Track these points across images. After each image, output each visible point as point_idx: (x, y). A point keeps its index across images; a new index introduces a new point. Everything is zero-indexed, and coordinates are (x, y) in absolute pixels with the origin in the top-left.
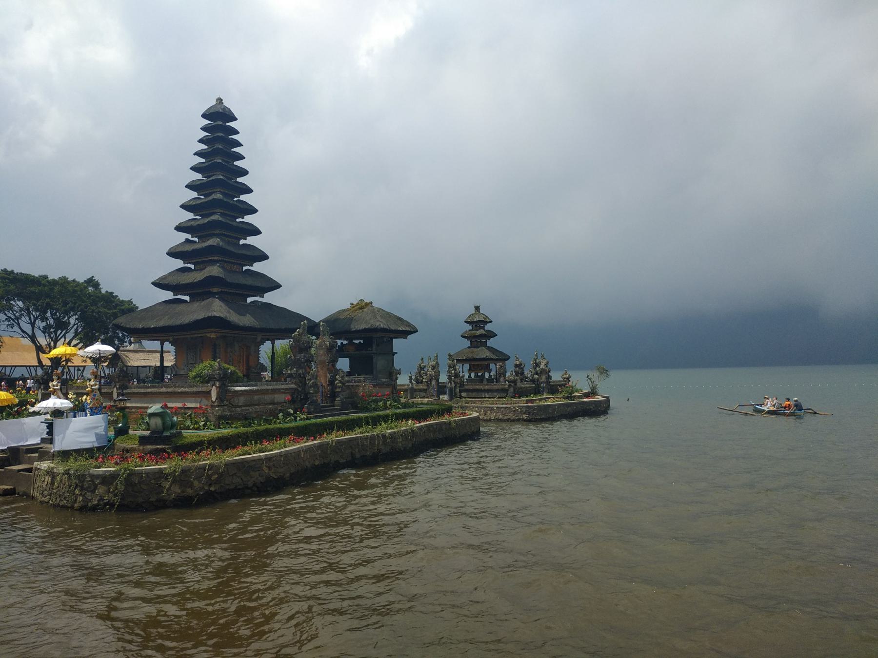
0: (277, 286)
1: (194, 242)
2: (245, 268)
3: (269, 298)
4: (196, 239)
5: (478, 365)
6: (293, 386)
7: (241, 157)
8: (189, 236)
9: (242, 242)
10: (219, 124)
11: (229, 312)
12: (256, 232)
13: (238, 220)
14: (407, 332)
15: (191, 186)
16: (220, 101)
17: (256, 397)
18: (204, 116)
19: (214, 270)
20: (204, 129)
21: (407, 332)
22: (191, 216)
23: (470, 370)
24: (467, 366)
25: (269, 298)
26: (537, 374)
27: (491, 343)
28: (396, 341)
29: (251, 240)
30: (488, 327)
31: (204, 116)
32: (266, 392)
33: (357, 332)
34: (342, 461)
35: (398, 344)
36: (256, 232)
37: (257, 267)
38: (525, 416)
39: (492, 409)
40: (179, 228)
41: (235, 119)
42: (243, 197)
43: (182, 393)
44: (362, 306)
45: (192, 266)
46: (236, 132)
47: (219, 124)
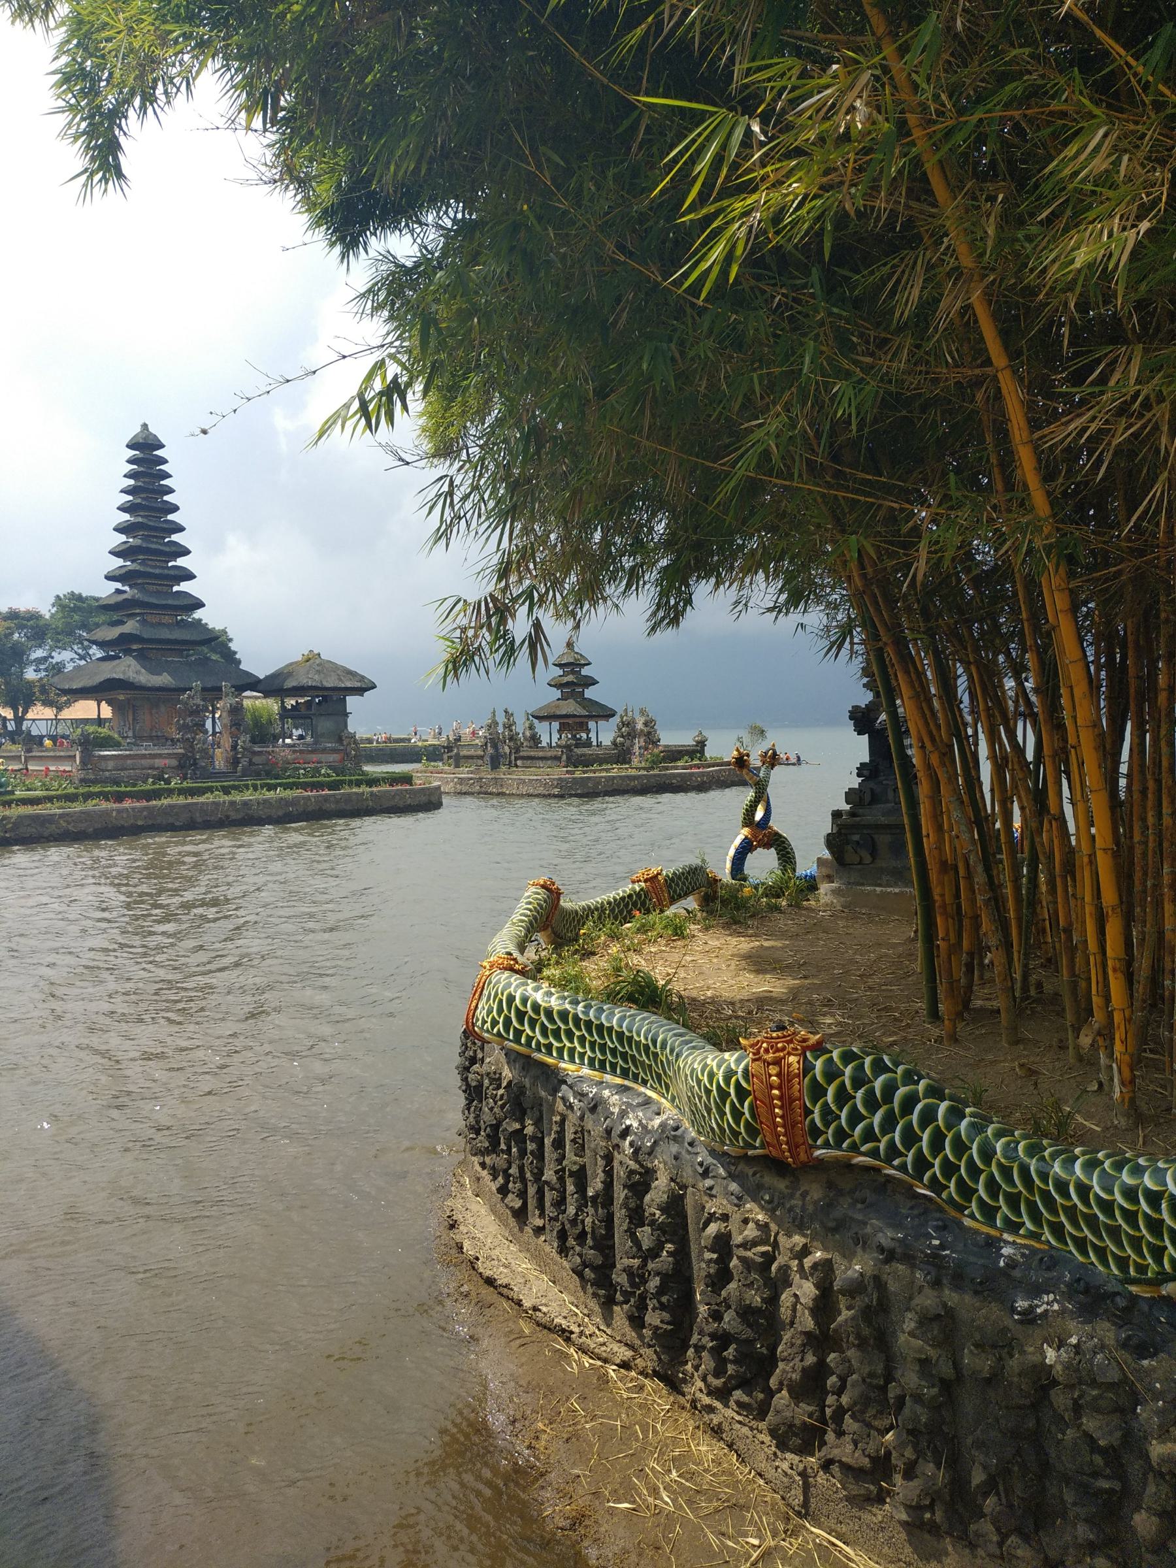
1: (125, 592)
4: (127, 588)
5: (572, 724)
6: (181, 751)
7: (170, 491)
8: (119, 585)
9: (175, 589)
10: (147, 454)
11: (138, 672)
12: (190, 576)
13: (170, 564)
14: (364, 687)
15: (119, 529)
16: (145, 426)
17: (129, 762)
18: (130, 446)
19: (130, 627)
20: (130, 461)
21: (364, 687)
22: (120, 562)
23: (560, 731)
24: (556, 725)
26: (623, 736)
27: (590, 693)
28: (350, 700)
29: (184, 586)
30: (585, 671)
31: (130, 446)
32: (144, 756)
33: (287, 690)
34: (177, 824)
35: (352, 702)
36: (190, 576)
38: (556, 791)
39: (523, 782)
40: (109, 578)
41: (162, 446)
42: (175, 537)
43: (61, 757)
44: (312, 659)
46: (165, 461)
47: (147, 454)
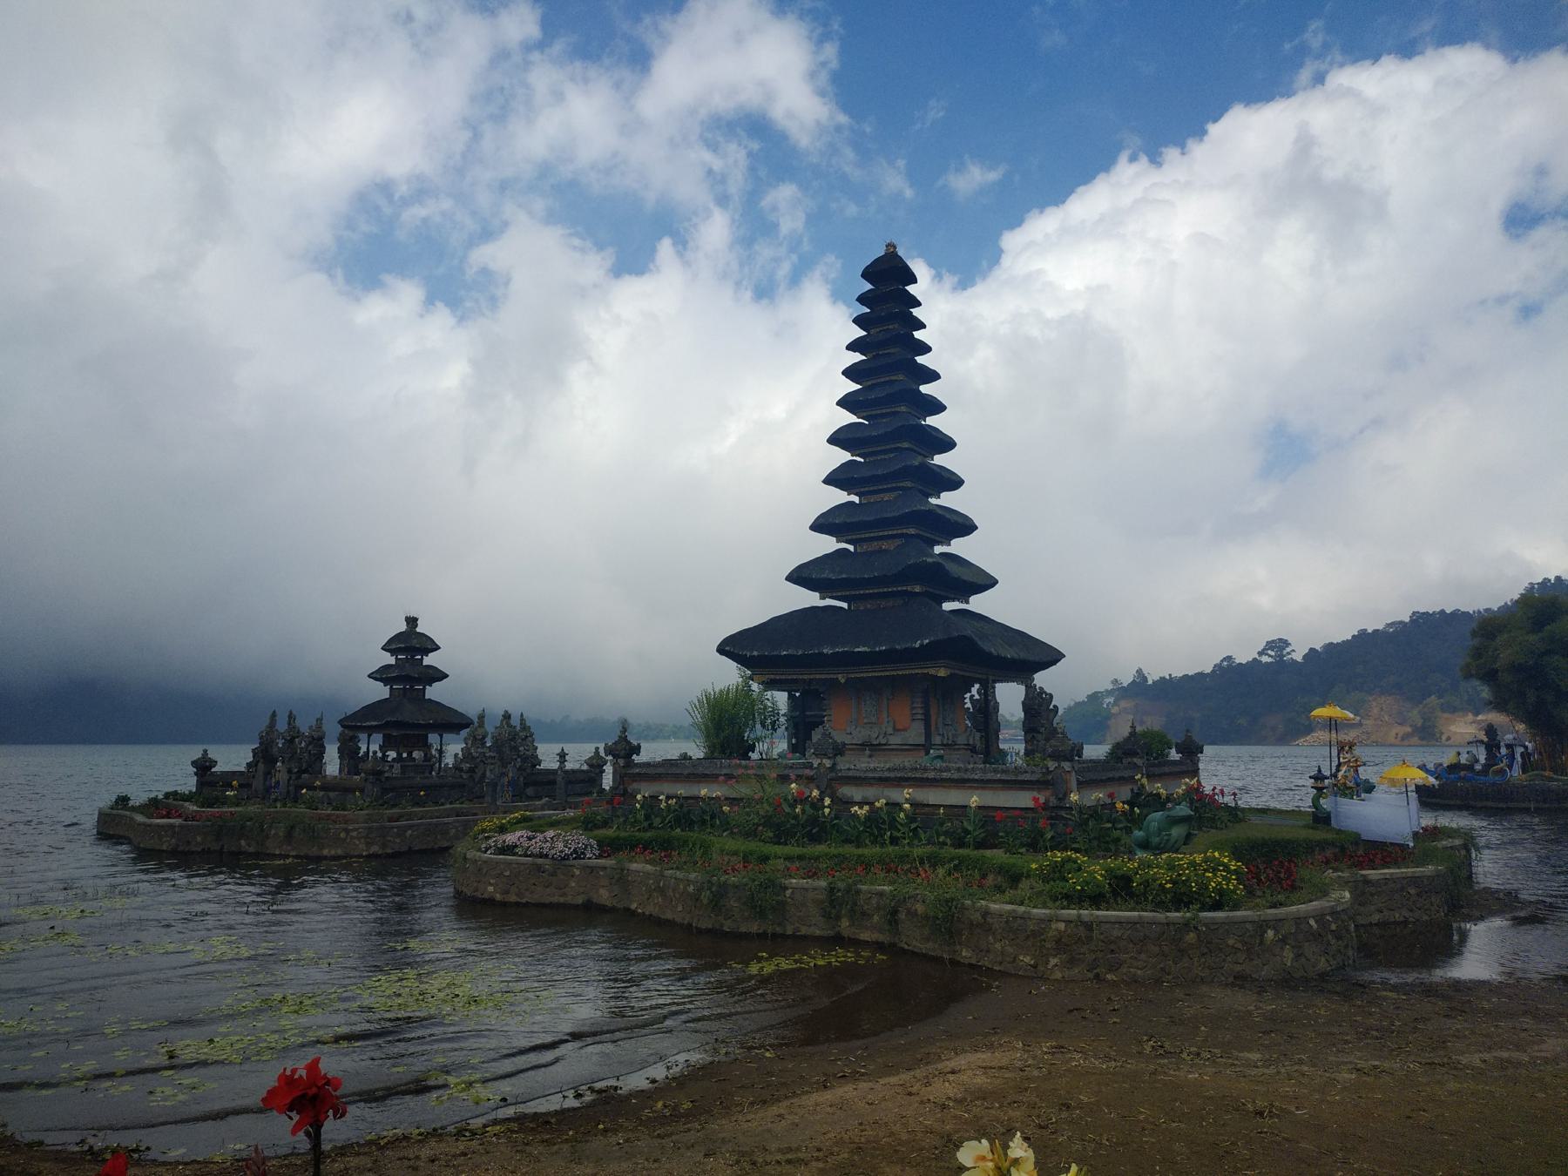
0: (991, 583)
2: (938, 549)
3: (979, 603)
4: (856, 499)
18: (866, 275)
25: (979, 603)
29: (947, 499)
31: (866, 275)
37: (958, 546)
45: (851, 548)
